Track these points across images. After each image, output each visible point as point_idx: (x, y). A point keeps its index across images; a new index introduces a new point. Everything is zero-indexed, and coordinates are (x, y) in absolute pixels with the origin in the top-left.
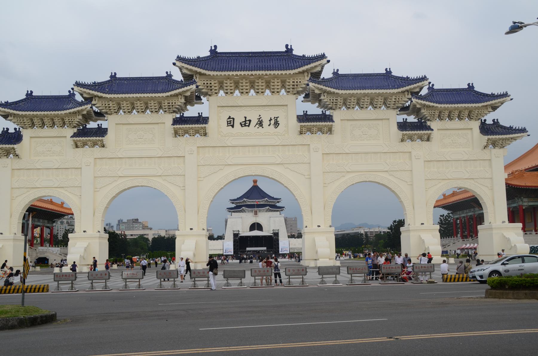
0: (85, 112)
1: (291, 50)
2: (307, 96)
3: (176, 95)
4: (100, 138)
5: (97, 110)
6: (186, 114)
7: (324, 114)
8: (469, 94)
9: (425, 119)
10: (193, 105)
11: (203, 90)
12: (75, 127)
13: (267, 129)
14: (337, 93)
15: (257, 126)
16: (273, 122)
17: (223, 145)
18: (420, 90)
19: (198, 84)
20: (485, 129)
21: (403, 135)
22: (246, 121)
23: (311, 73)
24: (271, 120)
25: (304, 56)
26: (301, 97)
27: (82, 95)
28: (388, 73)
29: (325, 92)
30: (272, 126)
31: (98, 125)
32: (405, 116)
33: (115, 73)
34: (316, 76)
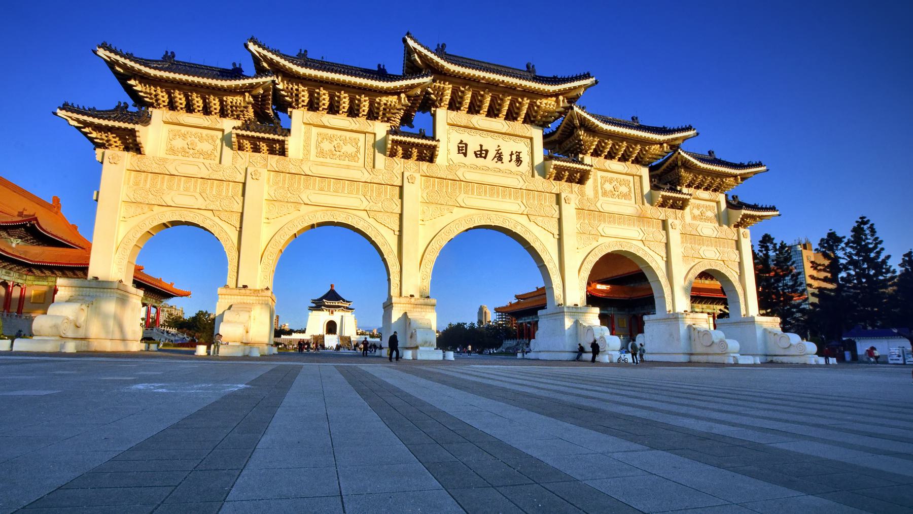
13: (508, 165)
16: (514, 157)
22: (481, 150)
24: (512, 154)
30: (513, 163)
33: (306, 51)
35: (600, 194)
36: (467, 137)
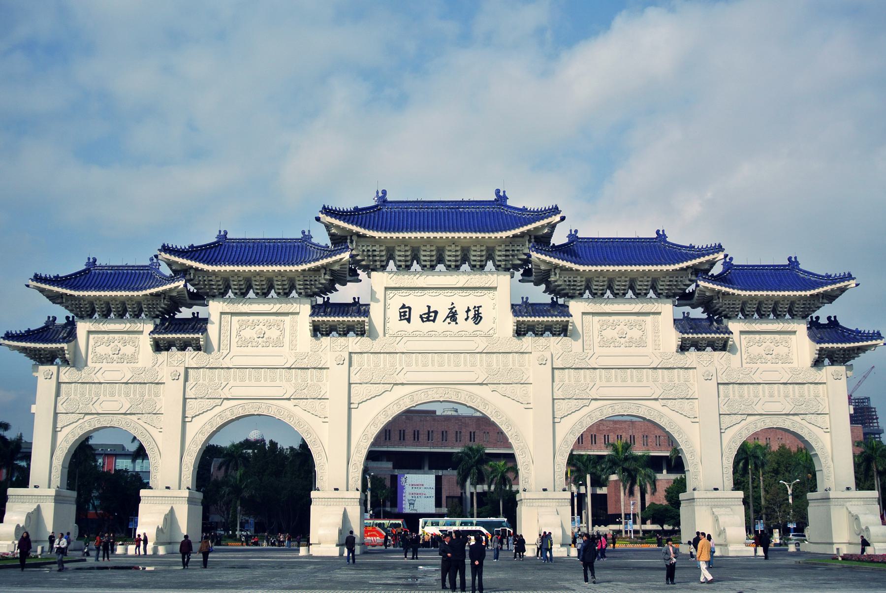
0: (175, 294)
1: (505, 198)
2: (527, 273)
3: (317, 270)
4: (196, 336)
5: (191, 288)
6: (335, 298)
7: (554, 304)
8: (788, 274)
9: (720, 314)
10: (344, 284)
11: (364, 263)
12: (157, 316)
13: (465, 325)
14: (577, 270)
15: (448, 320)
16: (471, 314)
18: (712, 267)
19: (354, 252)
20: (816, 330)
21: (683, 340)
22: (429, 312)
23: (536, 238)
24: (468, 310)
25: (525, 209)
26: (518, 275)
27: (170, 264)
28: (661, 236)
29: (556, 266)
30: (470, 321)
31: (193, 314)
32: (687, 309)
34: (542, 241)
35: (596, 345)
36: (410, 299)
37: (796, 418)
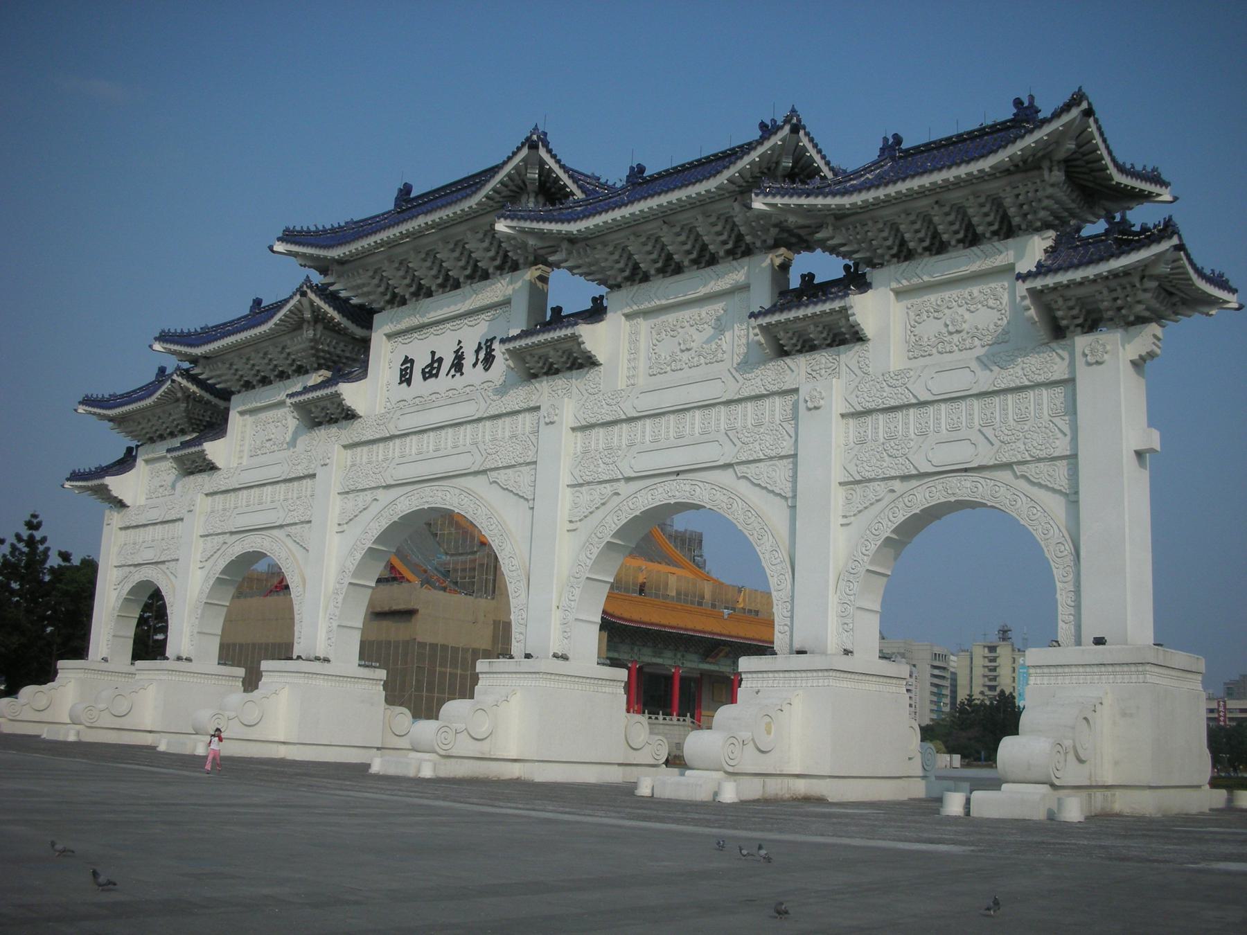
12: (193, 431)
15: (453, 372)
16: (482, 356)
17: (383, 435)
22: (433, 361)
30: (480, 366)
37: (1006, 476)
